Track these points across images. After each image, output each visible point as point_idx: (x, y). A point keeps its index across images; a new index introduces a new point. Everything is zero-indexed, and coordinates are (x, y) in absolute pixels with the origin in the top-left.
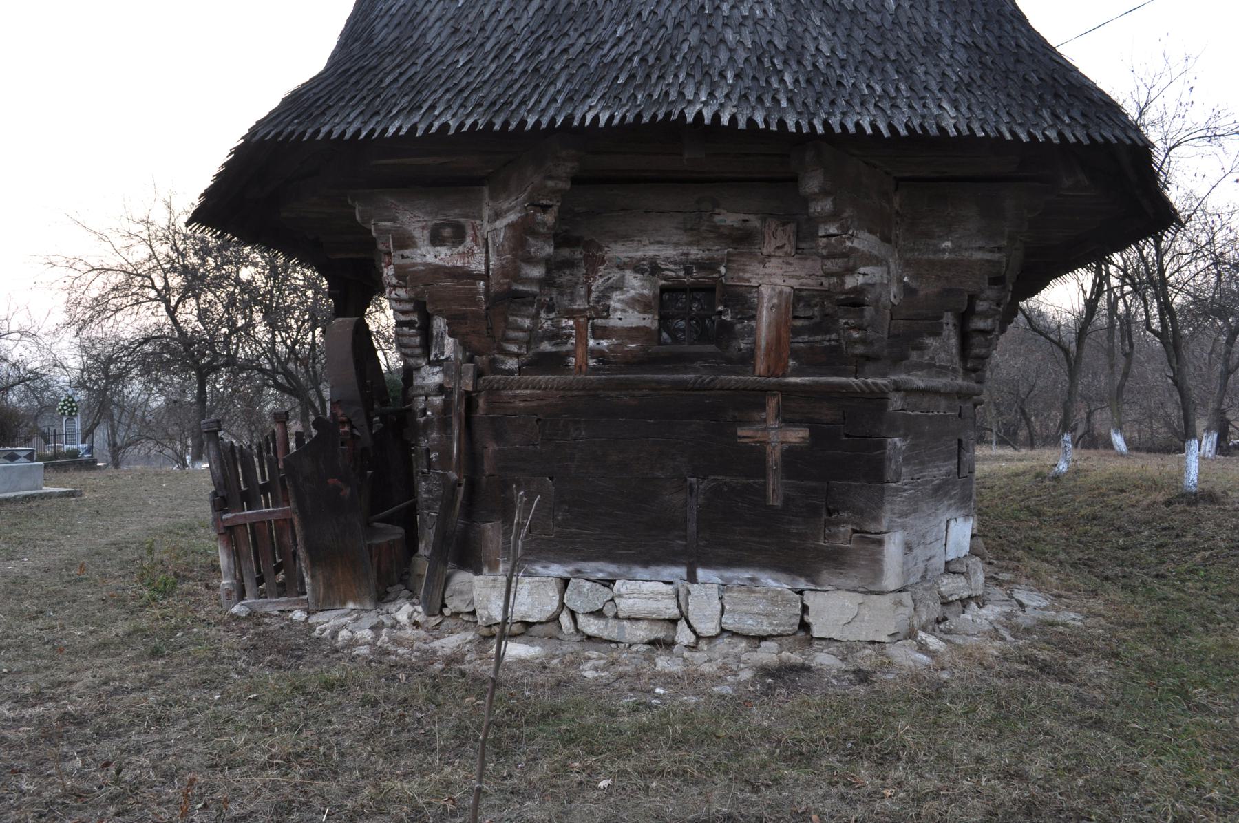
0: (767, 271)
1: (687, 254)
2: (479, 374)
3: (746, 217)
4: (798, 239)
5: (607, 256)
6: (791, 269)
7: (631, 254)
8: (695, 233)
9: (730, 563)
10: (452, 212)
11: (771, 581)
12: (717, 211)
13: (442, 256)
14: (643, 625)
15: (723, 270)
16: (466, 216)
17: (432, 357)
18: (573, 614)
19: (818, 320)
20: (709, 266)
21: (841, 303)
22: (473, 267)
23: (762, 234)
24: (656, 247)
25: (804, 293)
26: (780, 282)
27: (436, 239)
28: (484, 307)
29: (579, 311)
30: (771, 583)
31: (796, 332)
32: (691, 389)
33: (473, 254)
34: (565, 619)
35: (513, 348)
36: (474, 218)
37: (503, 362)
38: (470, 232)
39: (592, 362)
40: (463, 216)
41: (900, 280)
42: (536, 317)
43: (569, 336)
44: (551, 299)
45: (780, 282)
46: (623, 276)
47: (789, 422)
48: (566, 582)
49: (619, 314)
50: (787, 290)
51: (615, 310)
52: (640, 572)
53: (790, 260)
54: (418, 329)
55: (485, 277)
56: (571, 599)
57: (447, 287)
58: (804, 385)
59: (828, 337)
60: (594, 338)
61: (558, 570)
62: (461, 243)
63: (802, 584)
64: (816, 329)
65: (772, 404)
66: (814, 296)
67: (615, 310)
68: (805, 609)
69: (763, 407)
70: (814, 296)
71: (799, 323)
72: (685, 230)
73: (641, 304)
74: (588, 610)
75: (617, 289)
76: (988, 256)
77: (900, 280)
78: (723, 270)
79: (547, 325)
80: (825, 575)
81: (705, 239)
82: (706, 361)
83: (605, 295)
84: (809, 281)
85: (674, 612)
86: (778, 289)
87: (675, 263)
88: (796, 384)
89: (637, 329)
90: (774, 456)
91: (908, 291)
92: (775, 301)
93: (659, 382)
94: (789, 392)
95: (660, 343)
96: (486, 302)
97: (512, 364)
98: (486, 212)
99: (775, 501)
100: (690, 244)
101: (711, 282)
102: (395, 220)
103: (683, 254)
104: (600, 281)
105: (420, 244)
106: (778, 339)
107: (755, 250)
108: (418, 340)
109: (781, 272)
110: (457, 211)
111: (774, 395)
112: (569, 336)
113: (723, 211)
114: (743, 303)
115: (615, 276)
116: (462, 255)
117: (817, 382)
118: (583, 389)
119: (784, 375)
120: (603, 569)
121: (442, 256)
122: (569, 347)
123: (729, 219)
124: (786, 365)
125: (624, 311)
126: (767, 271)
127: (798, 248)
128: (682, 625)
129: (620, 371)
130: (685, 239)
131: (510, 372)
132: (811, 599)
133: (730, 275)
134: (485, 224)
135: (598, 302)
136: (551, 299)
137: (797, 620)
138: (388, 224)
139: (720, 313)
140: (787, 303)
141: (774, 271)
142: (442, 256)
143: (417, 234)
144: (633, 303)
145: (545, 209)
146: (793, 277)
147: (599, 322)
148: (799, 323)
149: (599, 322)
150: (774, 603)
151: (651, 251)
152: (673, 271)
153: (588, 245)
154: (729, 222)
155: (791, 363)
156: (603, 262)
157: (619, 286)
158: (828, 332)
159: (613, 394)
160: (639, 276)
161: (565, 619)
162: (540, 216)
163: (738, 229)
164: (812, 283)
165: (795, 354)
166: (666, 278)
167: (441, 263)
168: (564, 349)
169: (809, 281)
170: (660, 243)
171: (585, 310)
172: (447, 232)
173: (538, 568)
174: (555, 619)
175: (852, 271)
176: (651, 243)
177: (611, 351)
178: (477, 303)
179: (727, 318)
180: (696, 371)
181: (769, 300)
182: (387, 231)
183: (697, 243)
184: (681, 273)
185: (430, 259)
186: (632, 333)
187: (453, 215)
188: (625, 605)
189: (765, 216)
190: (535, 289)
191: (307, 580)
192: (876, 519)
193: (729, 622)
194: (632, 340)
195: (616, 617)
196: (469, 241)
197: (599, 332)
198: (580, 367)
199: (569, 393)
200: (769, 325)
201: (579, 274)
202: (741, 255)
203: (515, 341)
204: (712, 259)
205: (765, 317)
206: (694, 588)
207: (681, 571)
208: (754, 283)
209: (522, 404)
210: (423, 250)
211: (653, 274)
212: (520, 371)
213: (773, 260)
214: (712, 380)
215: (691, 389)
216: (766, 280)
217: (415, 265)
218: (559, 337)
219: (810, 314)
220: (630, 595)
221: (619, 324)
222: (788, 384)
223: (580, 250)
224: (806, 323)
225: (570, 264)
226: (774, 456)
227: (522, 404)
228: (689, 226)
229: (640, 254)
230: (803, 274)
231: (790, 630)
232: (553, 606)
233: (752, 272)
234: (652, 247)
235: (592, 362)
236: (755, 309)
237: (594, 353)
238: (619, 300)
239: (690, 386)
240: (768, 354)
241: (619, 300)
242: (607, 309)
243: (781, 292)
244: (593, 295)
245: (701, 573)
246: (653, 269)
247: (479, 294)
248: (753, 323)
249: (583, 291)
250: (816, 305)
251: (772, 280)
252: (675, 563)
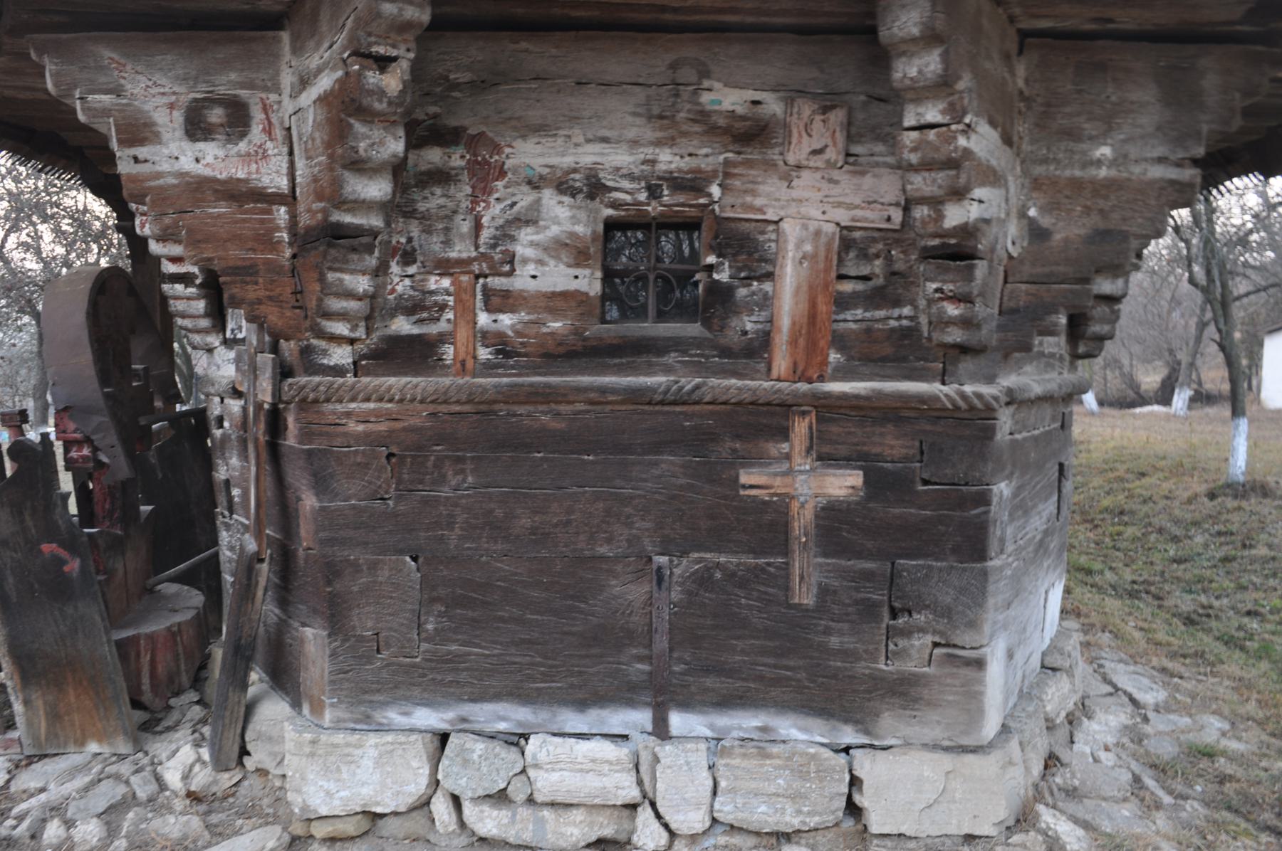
0: (795, 194)
1: (653, 162)
2: (284, 372)
3: (758, 96)
4: (850, 138)
5: (509, 164)
6: (836, 190)
7: (554, 161)
8: (666, 124)
9: (725, 702)
10: (224, 79)
11: (795, 731)
12: (706, 84)
13: (209, 159)
14: (578, 815)
15: (715, 191)
16: (251, 86)
17: (228, 334)
18: (456, 801)
19: (880, 281)
20: (692, 184)
21: (929, 255)
22: (266, 181)
23: (786, 126)
24: (598, 147)
25: (857, 234)
26: (816, 213)
27: (196, 128)
28: (288, 253)
29: (460, 262)
30: (795, 734)
31: (842, 302)
32: (662, 403)
33: (265, 157)
34: (441, 807)
35: (341, 328)
36: (266, 89)
37: (325, 353)
38: (257, 115)
39: (484, 354)
40: (243, 86)
41: (1022, 214)
42: (381, 271)
43: (443, 307)
44: (410, 240)
45: (816, 213)
46: (538, 201)
47: (828, 459)
48: (444, 738)
49: (531, 269)
50: (830, 228)
51: (525, 261)
52: (573, 720)
53: (836, 174)
54: (201, 286)
55: (290, 198)
56: (454, 776)
57: (219, 215)
58: (857, 397)
59: (896, 312)
60: (489, 309)
61: (429, 718)
62: (243, 135)
63: (849, 736)
64: (879, 297)
65: (801, 428)
66: (874, 240)
67: (525, 261)
68: (855, 782)
69: (784, 433)
70: (874, 240)
71: (847, 287)
72: (650, 118)
74: (481, 792)
75: (528, 223)
76: (1172, 173)
77: (1022, 214)
78: (715, 191)
79: (403, 286)
80: (887, 721)
81: (684, 134)
82: (685, 353)
83: (505, 234)
84: (868, 214)
85: (633, 794)
86: (813, 226)
87: (631, 177)
88: (844, 396)
89: (565, 295)
90: (803, 520)
91: (1037, 233)
92: (808, 248)
93: (603, 390)
94: (828, 408)
95: (604, 321)
96: (291, 244)
97: (341, 356)
98: (287, 79)
99: (805, 597)
100: (658, 143)
101: (693, 212)
102: (118, 91)
103: (644, 162)
104: (496, 209)
105: (166, 136)
106: (812, 316)
107: (774, 154)
108: (201, 305)
109: (819, 195)
110: (233, 76)
111: (804, 413)
112: (443, 307)
113: (717, 85)
114: (747, 247)
115: (525, 198)
116: (247, 157)
117: (879, 394)
118: (469, 402)
119: (821, 379)
121: (209, 159)
122: (442, 326)
123: (727, 99)
124: (825, 362)
125: (540, 262)
126: (795, 194)
127: (848, 155)
128: (645, 814)
129: (536, 370)
130: (650, 134)
131: (338, 371)
132: (865, 764)
133: (729, 200)
134: (286, 99)
135: (494, 246)
136: (410, 240)
137: (842, 803)
138: (106, 99)
139: (710, 268)
140: (828, 250)
141: (806, 194)
142: (211, 159)
143: (161, 117)
144: (558, 247)
145: (383, 63)
146: (839, 205)
147: (496, 282)
148: (847, 287)
149: (496, 282)
150: (803, 775)
151: (588, 155)
152: (630, 193)
153: (474, 142)
154: (727, 105)
155: (834, 356)
156: (502, 173)
157: (529, 219)
158: (897, 303)
159: (521, 410)
160: (567, 199)
161: (441, 807)
162: (373, 78)
163: (743, 118)
164: (872, 217)
165: (839, 341)
166: (615, 205)
167: (208, 172)
168: (433, 329)
169: (868, 214)
170: (605, 140)
171: (469, 261)
172: (216, 115)
173: (393, 716)
174: (424, 804)
175: (959, 194)
176: (588, 141)
177: (519, 334)
178: (274, 246)
179: (723, 276)
180: (668, 370)
181: (798, 246)
182: (106, 112)
183: (669, 142)
184: (643, 196)
185: (186, 164)
186: (557, 301)
187: (227, 83)
188: (546, 783)
189: (792, 94)
190: (376, 221)
191: (18, 707)
192: (973, 625)
193: (726, 809)
194: (555, 312)
195: (530, 800)
196: (256, 132)
197: (495, 301)
198: (463, 363)
199: (444, 408)
200: (797, 292)
201: (460, 195)
202: (749, 164)
203: (342, 316)
204: (698, 171)
206: (667, 751)
207: (642, 717)
208: (771, 215)
209: (361, 428)
210: (173, 148)
211: (591, 196)
212: (357, 369)
213: (805, 174)
214: (697, 387)
215: (662, 403)
216: (792, 210)
217: (159, 175)
218: (424, 308)
219: (865, 270)
220: (554, 765)
221: (532, 286)
222: (828, 395)
223: (460, 150)
224: (860, 286)
225: (442, 177)
226: (803, 520)
227: (361, 428)
228: (656, 110)
229: (567, 161)
230: (857, 201)
231: (830, 819)
232: (417, 785)
233: (768, 195)
234: (590, 148)
235: (484, 354)
236: (772, 262)
237: (486, 337)
238: (532, 244)
239: (658, 397)
240: (793, 342)
241: (532, 244)
242: (511, 259)
243: (818, 233)
244: (485, 235)
245: (678, 721)
247: (278, 229)
248: (767, 286)
249: (466, 227)
250: (877, 256)
251: (806, 207)
252: (631, 703)
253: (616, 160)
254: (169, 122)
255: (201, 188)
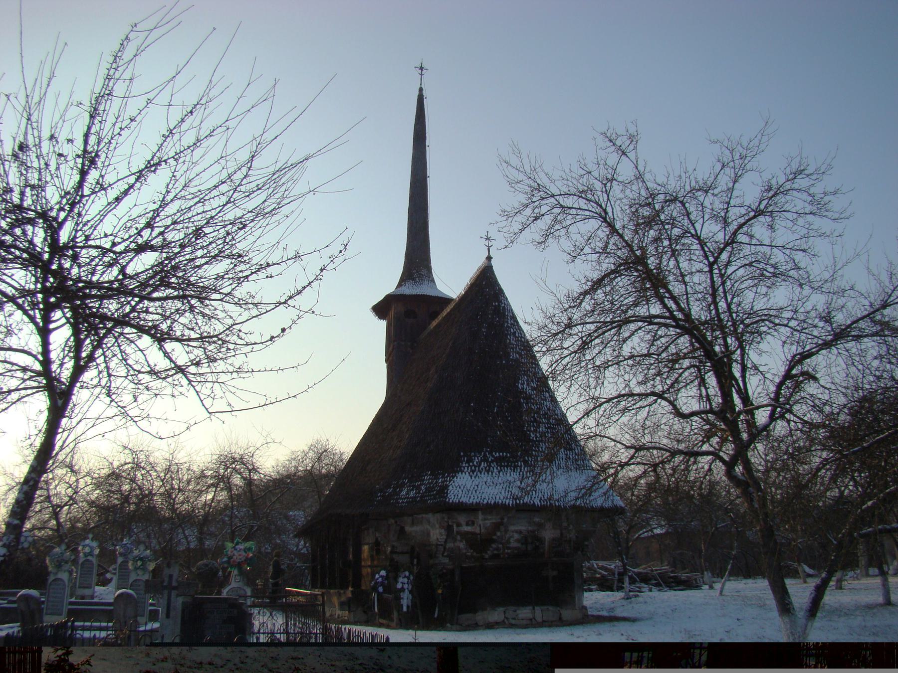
20: (533, 531)
27: (467, 525)
55: (480, 534)
73: (518, 541)
120: (514, 608)
186: (516, 548)
188: (520, 616)
193: (545, 618)
205: (547, 544)
237: (508, 553)
246: (520, 532)
253: (523, 528)
254: (463, 523)
255: (467, 533)
